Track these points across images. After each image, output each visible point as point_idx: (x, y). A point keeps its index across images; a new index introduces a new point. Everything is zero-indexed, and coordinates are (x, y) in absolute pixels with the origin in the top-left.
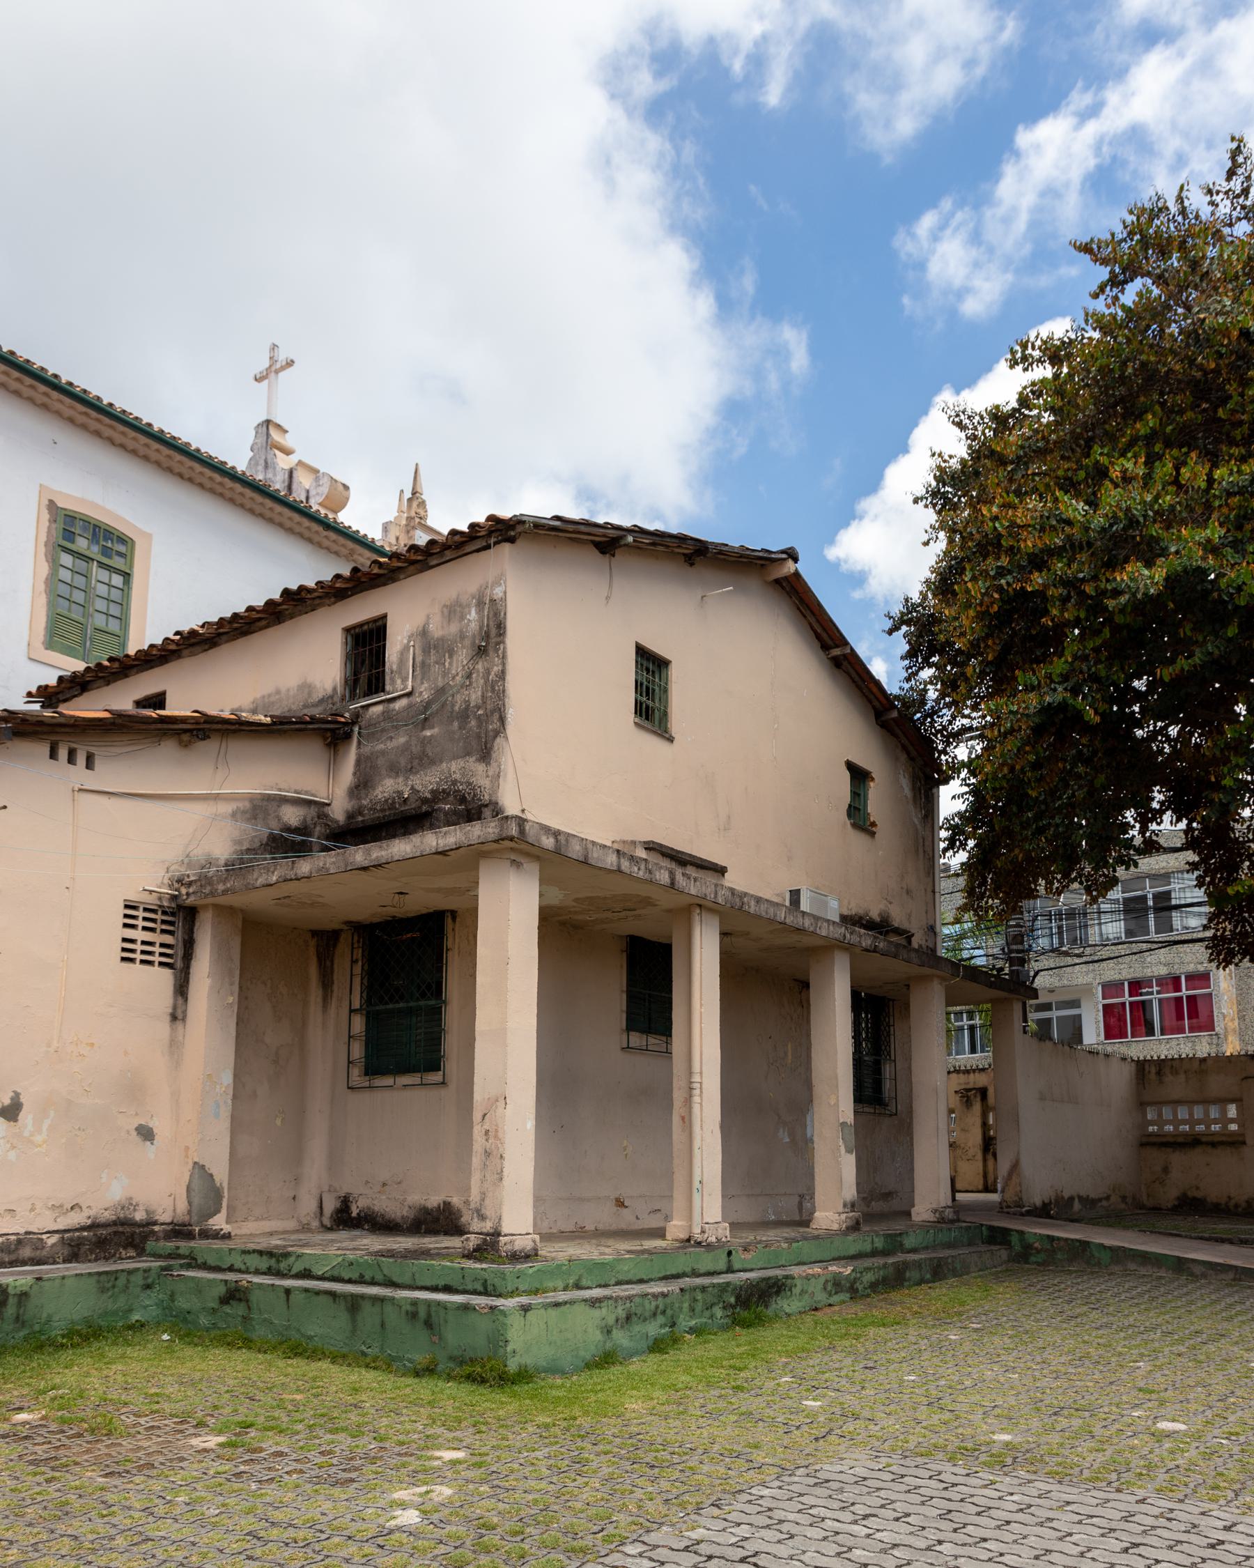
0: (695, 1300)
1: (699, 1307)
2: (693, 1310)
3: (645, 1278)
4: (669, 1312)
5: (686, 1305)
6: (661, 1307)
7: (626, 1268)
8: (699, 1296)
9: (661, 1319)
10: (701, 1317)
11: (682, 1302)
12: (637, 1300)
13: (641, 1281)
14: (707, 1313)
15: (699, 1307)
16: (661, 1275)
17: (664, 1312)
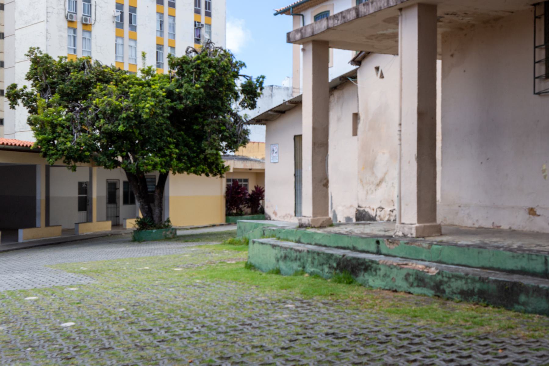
0: (314, 258)
1: (316, 262)
2: (313, 263)
3: (328, 245)
4: (302, 260)
5: (310, 259)
6: (298, 257)
7: (318, 238)
8: (316, 257)
9: (298, 263)
10: (317, 268)
11: (308, 257)
12: (289, 250)
13: (325, 246)
14: (320, 267)
15: (316, 262)
16: (336, 245)
17: (300, 260)
